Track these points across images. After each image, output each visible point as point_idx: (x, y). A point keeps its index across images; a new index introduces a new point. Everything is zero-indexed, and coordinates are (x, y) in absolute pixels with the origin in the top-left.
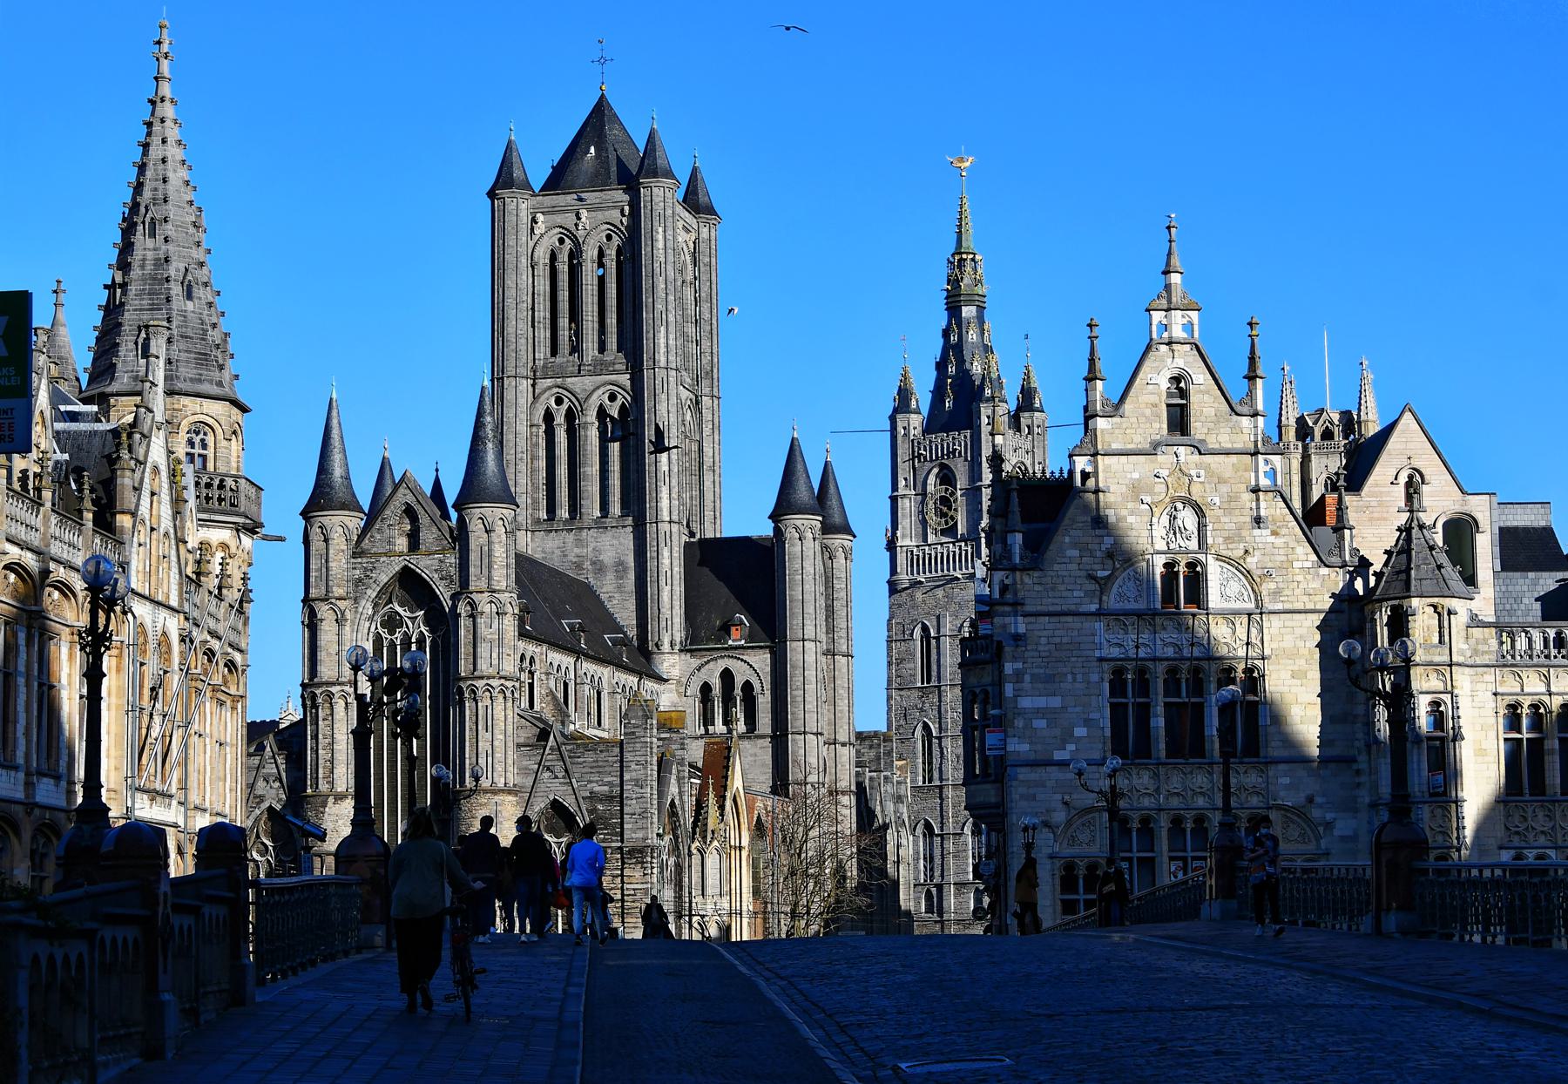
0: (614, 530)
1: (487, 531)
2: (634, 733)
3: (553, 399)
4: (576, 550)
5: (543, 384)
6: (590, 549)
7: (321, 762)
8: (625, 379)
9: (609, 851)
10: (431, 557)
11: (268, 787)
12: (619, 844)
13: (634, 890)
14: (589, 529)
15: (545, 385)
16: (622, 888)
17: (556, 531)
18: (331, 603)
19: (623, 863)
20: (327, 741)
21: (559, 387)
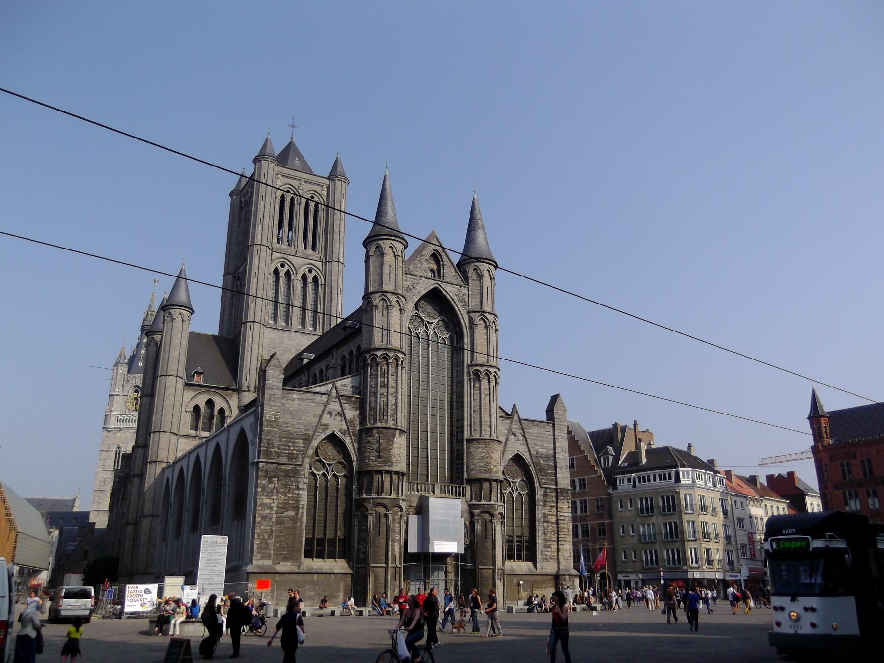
0: (308, 335)
1: (491, 279)
2: (560, 419)
3: (279, 265)
4: (288, 342)
5: (276, 255)
6: (296, 342)
7: (390, 404)
8: (319, 264)
9: (548, 490)
10: (453, 286)
11: (333, 419)
12: (554, 487)
13: (564, 516)
14: (296, 332)
15: (277, 256)
16: (557, 516)
17: (278, 329)
18: (398, 297)
19: (557, 499)
20: (393, 390)
21: (285, 259)
